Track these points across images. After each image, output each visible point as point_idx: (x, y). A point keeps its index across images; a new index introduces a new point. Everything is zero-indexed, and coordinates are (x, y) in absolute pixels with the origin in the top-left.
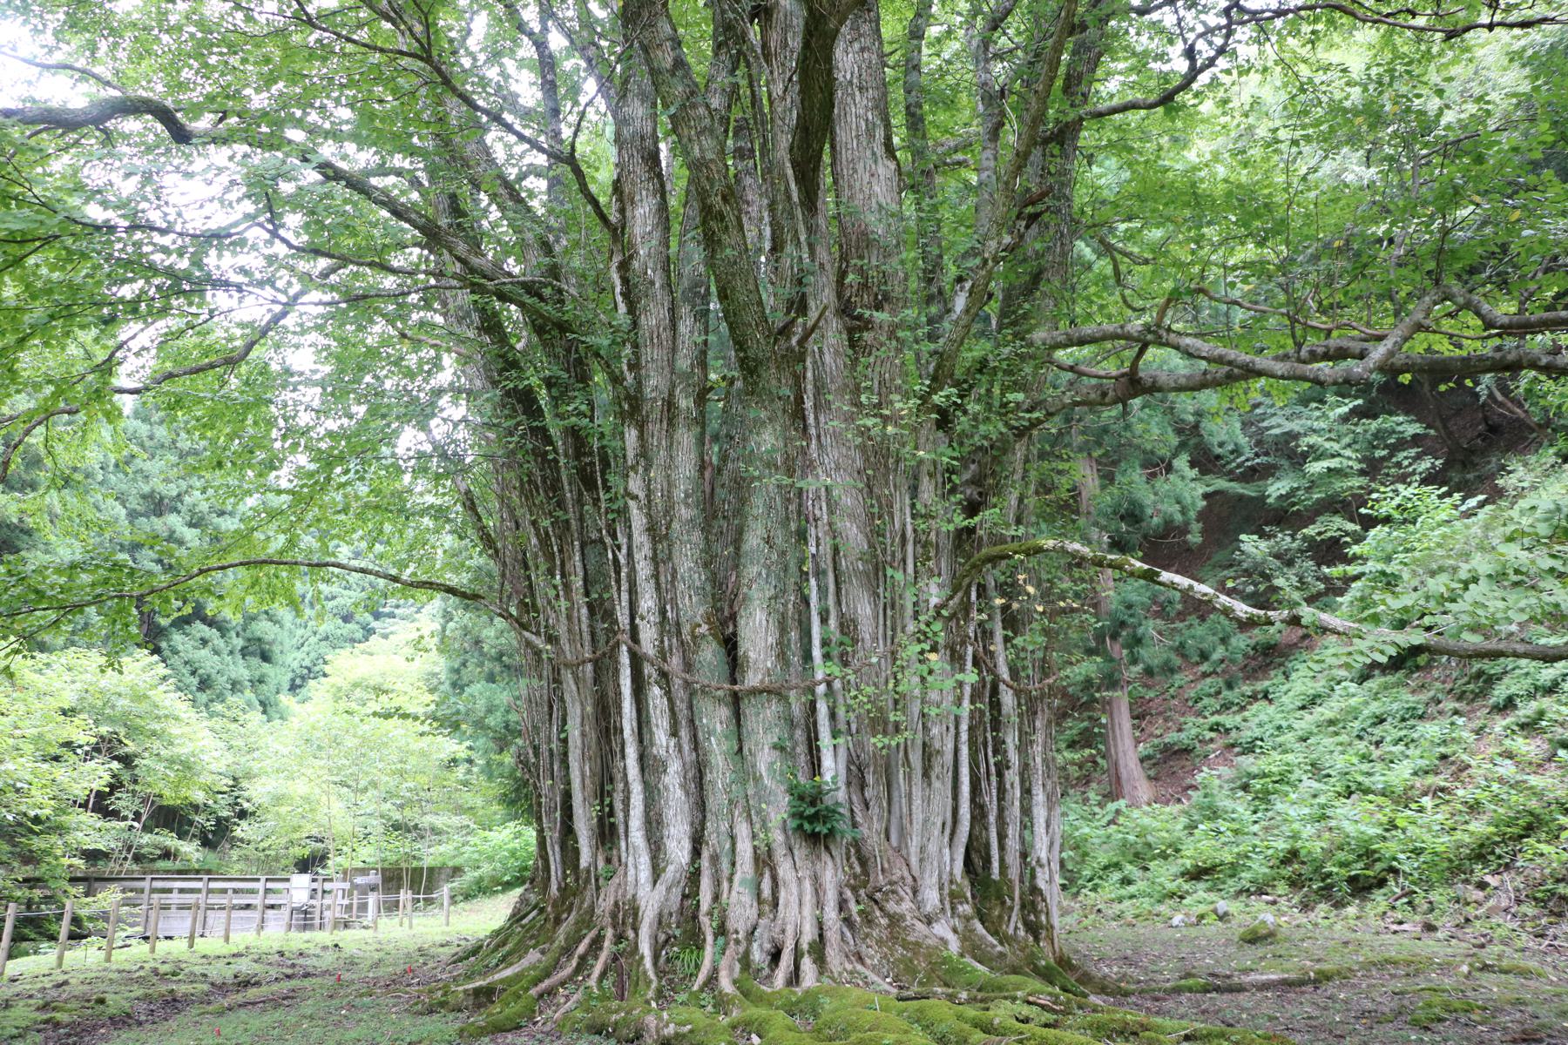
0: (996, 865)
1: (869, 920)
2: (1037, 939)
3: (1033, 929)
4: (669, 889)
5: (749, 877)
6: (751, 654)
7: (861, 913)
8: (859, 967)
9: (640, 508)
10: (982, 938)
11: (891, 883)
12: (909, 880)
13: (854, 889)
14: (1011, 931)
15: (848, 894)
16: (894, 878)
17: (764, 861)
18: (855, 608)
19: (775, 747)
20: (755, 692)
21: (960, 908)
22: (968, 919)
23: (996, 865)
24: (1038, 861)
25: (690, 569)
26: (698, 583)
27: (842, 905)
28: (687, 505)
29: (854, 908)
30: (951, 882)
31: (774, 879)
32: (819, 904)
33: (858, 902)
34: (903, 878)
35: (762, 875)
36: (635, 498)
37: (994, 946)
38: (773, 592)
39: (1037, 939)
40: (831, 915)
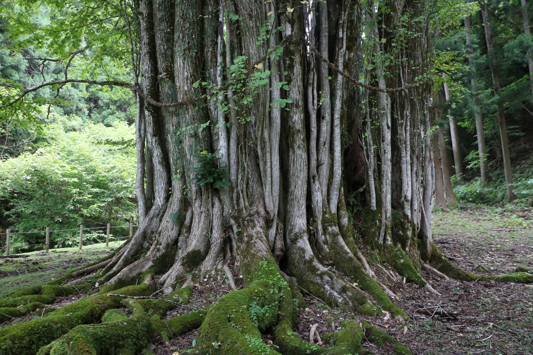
0: (374, 201)
1: (241, 240)
2: (404, 247)
3: (400, 240)
4: (151, 219)
5: (174, 212)
6: (178, 84)
7: (239, 233)
8: (226, 268)
9: (143, 19)
10: (342, 247)
11: (250, 215)
12: (263, 212)
13: (236, 219)
14: (381, 241)
15: (232, 222)
16: (252, 212)
17: (186, 203)
18: (249, 50)
19: (191, 136)
20: (182, 104)
21: (330, 229)
22: (334, 235)
23: (374, 201)
24: (406, 197)
25: (160, 44)
26: (163, 51)
27: (226, 228)
28: (159, 10)
29: (235, 230)
30: (324, 213)
31: (192, 212)
32: (210, 229)
33: (239, 226)
34: (258, 213)
35: (186, 210)
36: (141, 14)
37: (347, 253)
38: (187, 45)
39: (404, 247)
40: (217, 235)
